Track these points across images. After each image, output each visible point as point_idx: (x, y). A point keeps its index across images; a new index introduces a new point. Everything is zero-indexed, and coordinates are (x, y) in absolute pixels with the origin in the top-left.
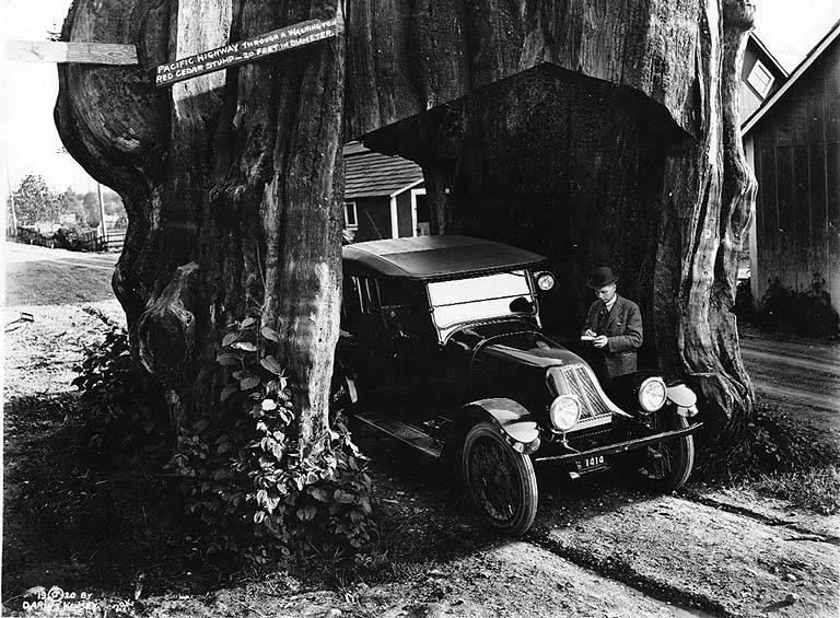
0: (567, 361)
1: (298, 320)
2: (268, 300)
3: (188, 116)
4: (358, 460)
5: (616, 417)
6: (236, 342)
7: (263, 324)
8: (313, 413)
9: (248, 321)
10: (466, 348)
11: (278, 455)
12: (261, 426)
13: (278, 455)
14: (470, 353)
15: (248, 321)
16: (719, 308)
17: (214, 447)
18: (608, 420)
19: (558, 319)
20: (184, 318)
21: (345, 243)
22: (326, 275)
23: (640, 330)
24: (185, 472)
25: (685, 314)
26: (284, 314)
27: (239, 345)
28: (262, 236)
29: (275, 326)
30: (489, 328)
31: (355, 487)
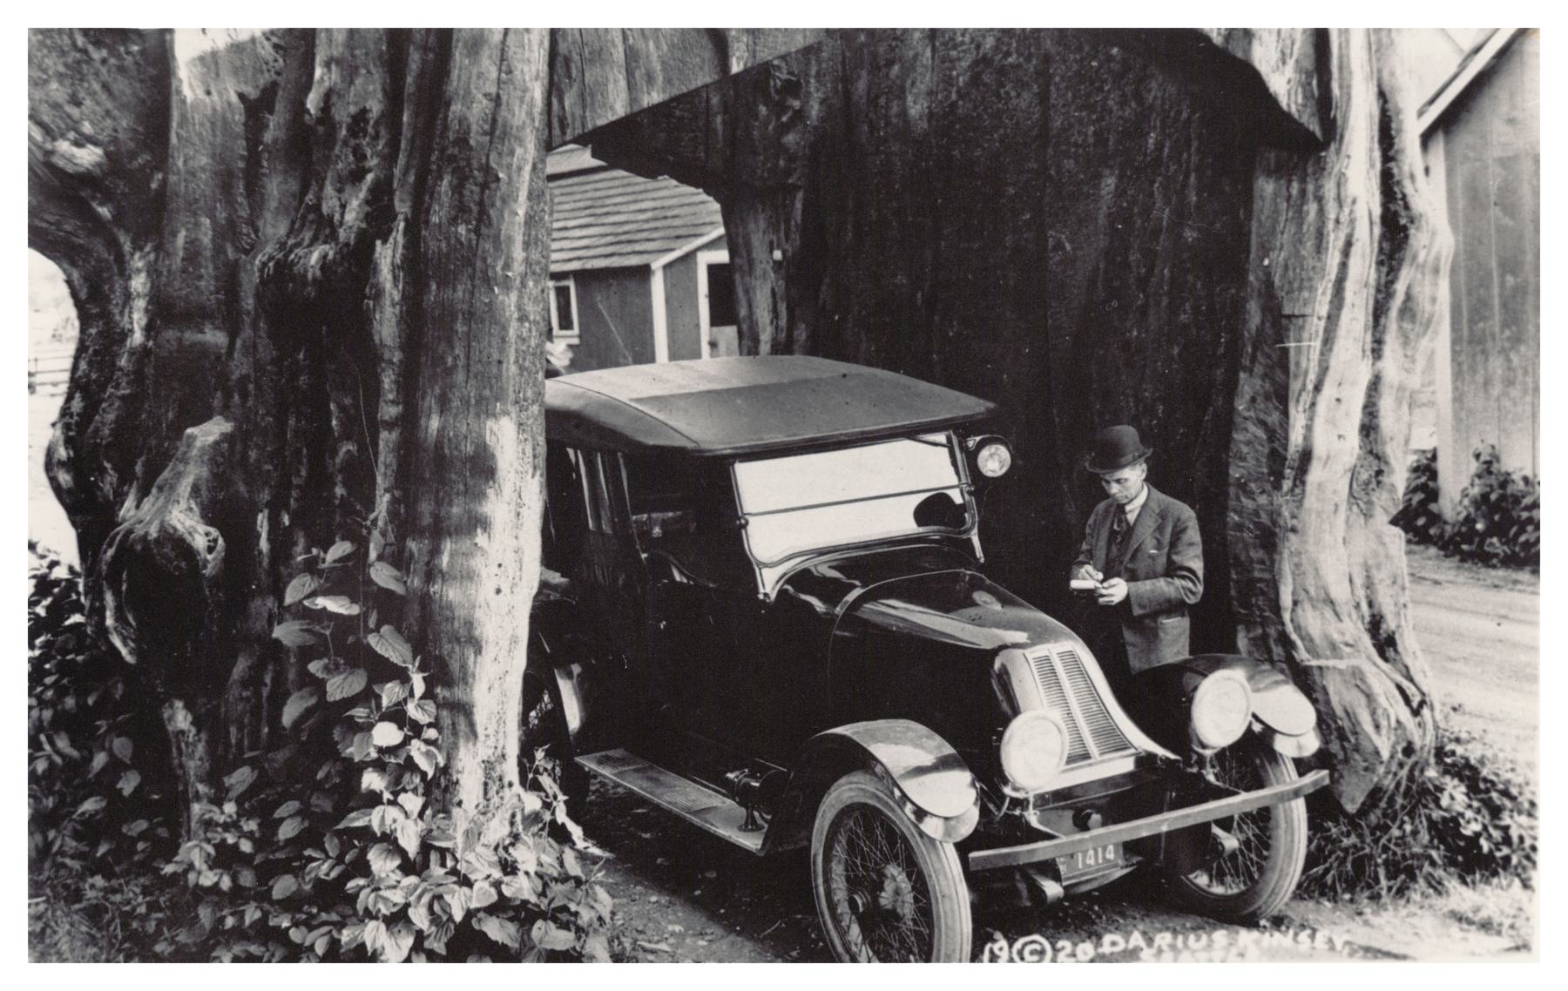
0: (1039, 636)
1: (448, 546)
2: (383, 502)
3: (208, 93)
4: (583, 857)
5: (1144, 761)
6: (313, 594)
7: (373, 555)
8: (484, 750)
9: (340, 549)
10: (819, 606)
11: (411, 844)
12: (372, 781)
13: (411, 844)
14: (829, 619)
15: (340, 549)
16: (1368, 515)
17: (270, 826)
18: (1123, 765)
19: (1019, 541)
20: (200, 542)
21: (552, 373)
22: (512, 444)
23: (1198, 565)
24: (208, 879)
25: (1294, 530)
26: (419, 533)
27: (321, 602)
28: (370, 356)
29: (398, 559)
30: (874, 565)
31: (576, 914)
